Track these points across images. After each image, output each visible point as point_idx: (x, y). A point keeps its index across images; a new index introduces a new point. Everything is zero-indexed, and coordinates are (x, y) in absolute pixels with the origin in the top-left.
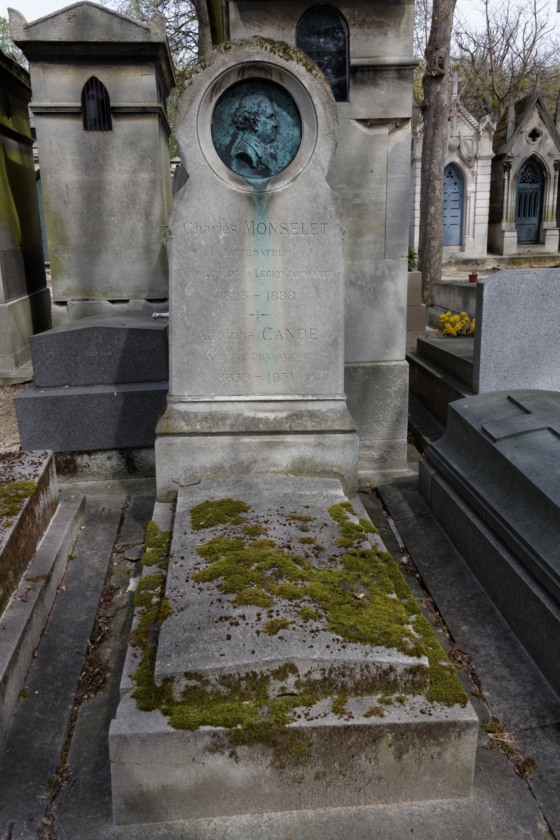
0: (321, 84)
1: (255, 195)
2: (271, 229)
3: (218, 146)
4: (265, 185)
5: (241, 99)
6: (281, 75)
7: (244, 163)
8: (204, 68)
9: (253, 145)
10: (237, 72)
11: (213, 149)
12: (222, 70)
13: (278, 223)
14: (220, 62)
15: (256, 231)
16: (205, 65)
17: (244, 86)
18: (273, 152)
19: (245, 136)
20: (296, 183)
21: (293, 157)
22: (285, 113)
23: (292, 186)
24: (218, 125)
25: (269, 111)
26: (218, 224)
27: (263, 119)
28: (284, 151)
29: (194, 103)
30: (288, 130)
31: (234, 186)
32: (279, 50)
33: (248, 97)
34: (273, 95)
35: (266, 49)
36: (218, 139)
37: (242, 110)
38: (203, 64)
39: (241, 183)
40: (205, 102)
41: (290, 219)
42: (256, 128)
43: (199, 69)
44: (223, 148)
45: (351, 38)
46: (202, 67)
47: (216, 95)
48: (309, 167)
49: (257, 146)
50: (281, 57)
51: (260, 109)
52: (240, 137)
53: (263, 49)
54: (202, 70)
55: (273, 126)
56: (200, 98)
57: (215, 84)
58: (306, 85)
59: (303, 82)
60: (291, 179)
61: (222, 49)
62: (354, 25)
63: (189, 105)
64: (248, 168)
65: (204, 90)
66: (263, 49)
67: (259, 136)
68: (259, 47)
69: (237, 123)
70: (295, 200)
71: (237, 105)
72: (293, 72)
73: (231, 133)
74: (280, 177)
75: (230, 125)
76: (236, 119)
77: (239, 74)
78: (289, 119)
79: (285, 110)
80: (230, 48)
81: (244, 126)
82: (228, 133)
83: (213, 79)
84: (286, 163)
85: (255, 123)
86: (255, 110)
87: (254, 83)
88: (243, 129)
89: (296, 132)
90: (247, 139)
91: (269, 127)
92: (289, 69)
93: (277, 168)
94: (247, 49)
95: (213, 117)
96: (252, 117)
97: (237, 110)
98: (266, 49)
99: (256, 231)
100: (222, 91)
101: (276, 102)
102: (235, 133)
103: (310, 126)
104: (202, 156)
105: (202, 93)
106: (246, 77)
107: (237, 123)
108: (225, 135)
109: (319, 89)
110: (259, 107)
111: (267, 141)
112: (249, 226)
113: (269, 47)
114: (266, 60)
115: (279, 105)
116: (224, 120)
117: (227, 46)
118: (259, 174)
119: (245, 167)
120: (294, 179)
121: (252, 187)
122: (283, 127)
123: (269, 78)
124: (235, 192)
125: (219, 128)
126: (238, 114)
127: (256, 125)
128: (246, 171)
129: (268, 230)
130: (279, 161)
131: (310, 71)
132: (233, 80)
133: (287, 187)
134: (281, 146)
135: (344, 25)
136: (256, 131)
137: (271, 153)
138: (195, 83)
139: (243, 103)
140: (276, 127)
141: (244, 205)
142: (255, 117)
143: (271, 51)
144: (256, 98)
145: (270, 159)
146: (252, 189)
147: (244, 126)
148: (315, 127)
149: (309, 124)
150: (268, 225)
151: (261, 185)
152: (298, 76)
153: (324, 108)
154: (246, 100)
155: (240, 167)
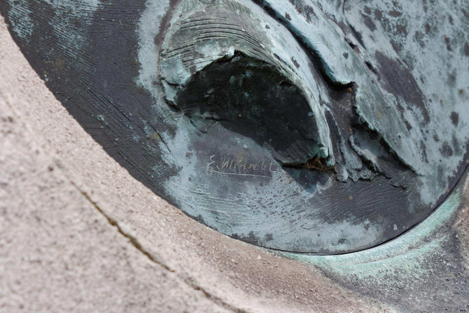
7: (244, 144)
28: (435, 45)
44: (74, 40)
64: (282, 180)
118: (360, 215)
130: (434, 108)
155: (231, 177)
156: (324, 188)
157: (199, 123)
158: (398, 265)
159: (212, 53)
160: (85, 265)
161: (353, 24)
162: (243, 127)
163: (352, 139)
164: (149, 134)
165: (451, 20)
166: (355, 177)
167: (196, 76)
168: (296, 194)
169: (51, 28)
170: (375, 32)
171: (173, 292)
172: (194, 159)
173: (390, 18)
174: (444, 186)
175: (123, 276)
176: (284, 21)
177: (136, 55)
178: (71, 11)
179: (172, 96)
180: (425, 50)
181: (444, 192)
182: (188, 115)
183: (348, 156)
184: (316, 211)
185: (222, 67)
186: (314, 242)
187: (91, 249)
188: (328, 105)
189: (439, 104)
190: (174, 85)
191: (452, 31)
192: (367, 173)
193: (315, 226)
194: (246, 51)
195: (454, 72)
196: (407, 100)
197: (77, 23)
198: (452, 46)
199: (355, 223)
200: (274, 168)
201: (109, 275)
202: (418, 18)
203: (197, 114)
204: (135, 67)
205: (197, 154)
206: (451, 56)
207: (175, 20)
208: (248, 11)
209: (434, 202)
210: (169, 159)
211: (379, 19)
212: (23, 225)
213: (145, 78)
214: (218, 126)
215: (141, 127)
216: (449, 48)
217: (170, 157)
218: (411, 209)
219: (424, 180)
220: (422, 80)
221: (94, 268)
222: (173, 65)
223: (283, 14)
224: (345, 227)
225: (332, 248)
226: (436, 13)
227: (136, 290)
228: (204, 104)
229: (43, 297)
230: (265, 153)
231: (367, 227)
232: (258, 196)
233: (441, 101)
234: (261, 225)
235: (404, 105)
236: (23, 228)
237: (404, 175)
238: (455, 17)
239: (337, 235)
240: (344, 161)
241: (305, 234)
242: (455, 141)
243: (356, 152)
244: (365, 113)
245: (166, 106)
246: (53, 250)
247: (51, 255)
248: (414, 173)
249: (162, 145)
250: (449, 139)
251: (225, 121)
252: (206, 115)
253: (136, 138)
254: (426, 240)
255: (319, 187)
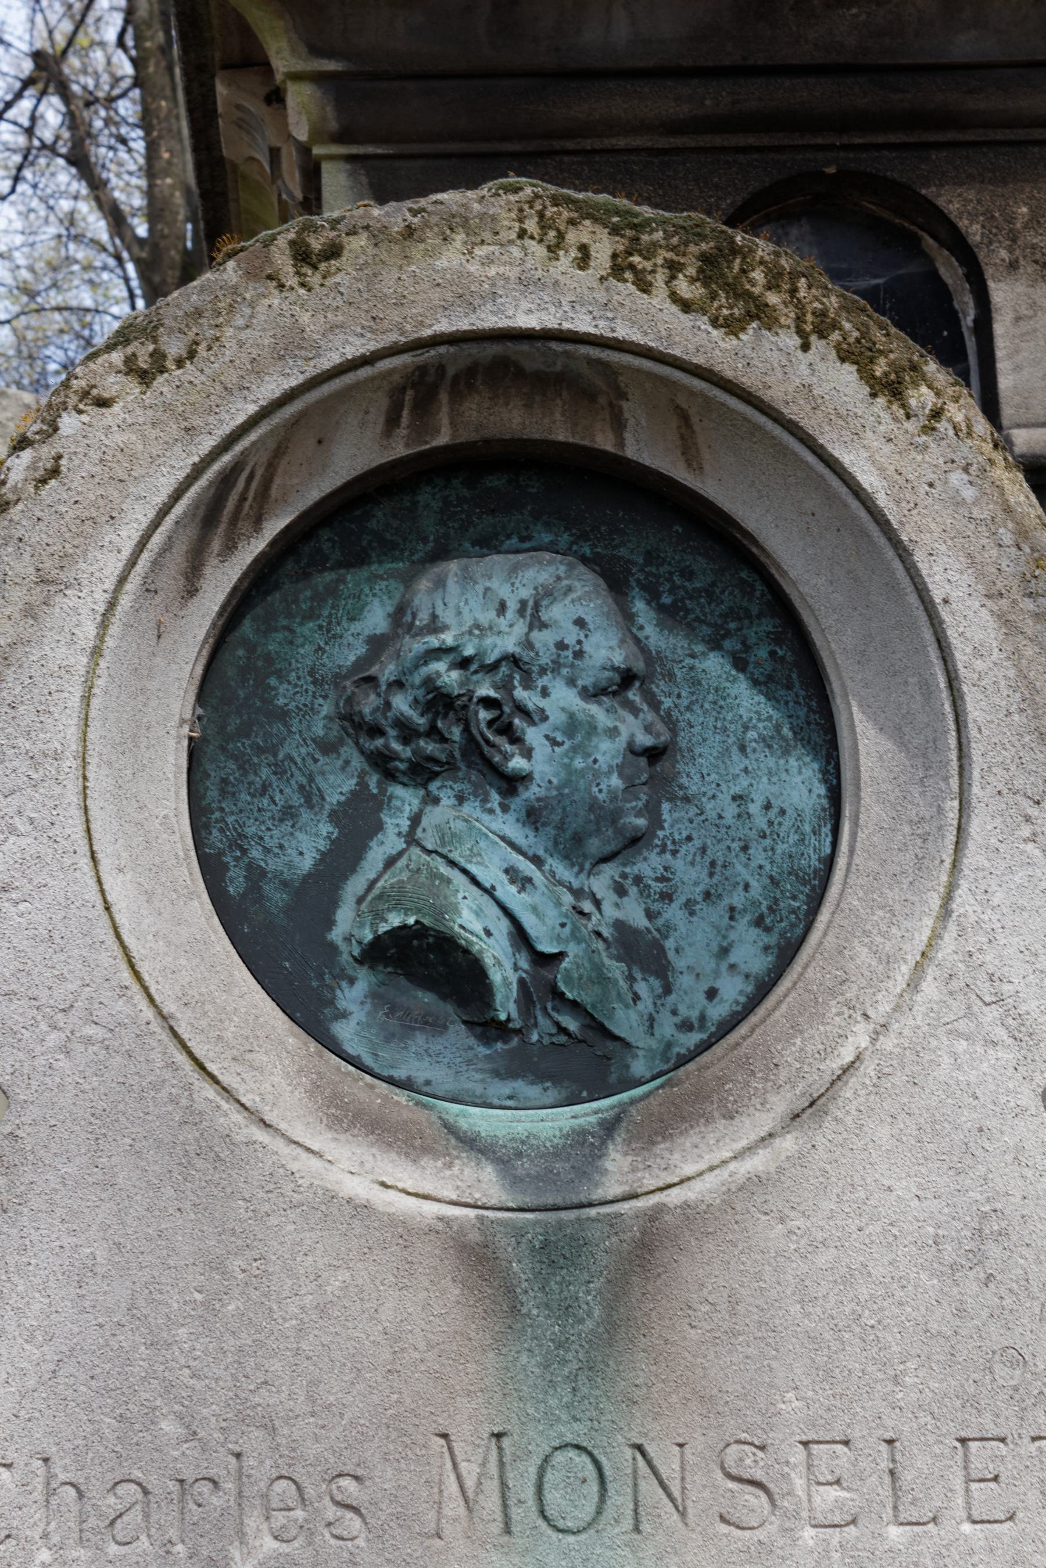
0: (980, 475)
1: (518, 1232)
2: (649, 1486)
3: (236, 883)
4: (586, 1149)
5: (408, 580)
6: (684, 417)
7: (426, 998)
8: (145, 378)
9: (490, 874)
10: (381, 403)
11: (200, 909)
12: (272, 388)
13: (698, 1444)
14: (261, 338)
15: (524, 1514)
16: (158, 356)
17: (428, 498)
18: (638, 919)
19: (433, 817)
20: (825, 1134)
21: (786, 954)
22: (714, 665)
23: (799, 1159)
24: (243, 745)
25: (606, 650)
26: (222, 1466)
27: (561, 699)
28: (716, 913)
29: (71, 599)
30: (743, 766)
31: (356, 1171)
32: (674, 268)
33: (453, 567)
34: (629, 553)
35: (584, 259)
36: (238, 843)
37: (416, 646)
38: (143, 351)
39: (409, 1143)
40: (149, 590)
41: (791, 1405)
42: (518, 763)
43: (112, 384)
44: (277, 897)
45: (1000, 328)
46: (130, 367)
47: (230, 548)
48: (918, 1017)
49: (524, 882)
50: (686, 306)
51: (544, 639)
52: (395, 823)
53: (565, 261)
54: (133, 387)
55: (632, 750)
56: (114, 566)
57: (226, 480)
58: (868, 479)
59: (847, 458)
60: (781, 1104)
61: (282, 259)
62: (1013, 266)
63: (29, 612)
64: (458, 1035)
65: (141, 516)
66: (565, 261)
67: (533, 817)
68: (539, 251)
69: (376, 731)
70: (824, 1259)
71: (376, 618)
72: (775, 394)
73: (334, 798)
74: (700, 1096)
75: (328, 748)
76: (368, 705)
77: (392, 421)
78: (747, 700)
79: (715, 644)
80: (334, 251)
81: (430, 747)
82: (311, 796)
83: (208, 444)
84: (733, 991)
85: (507, 731)
86: (509, 644)
87: (495, 482)
88: (422, 773)
89: (800, 785)
90: (447, 836)
91: (607, 752)
92: (749, 380)
93: (667, 1027)
94: (450, 258)
95: (201, 697)
96: (485, 690)
97: (378, 645)
98: (584, 259)
99: (524, 1514)
100: (275, 526)
101: (653, 596)
102: (360, 795)
103: (902, 744)
104: (109, 957)
105: (129, 535)
106: (443, 439)
107: (376, 731)
108: (288, 813)
109: (959, 503)
110: (537, 623)
111: (594, 846)
112: (470, 1471)
113: (604, 247)
114: (583, 324)
115: (671, 615)
116: (283, 715)
117: (316, 244)
118: (540, 1076)
119: (435, 1026)
120: (811, 1109)
121: (489, 1172)
122: (707, 753)
123: (604, 441)
124: (362, 1209)
125: (245, 766)
126: (388, 672)
127: (516, 739)
128: (443, 1056)
129: (620, 1499)
130: (685, 981)
131: (891, 388)
132: (355, 453)
133: (757, 1163)
134: (690, 876)
135: (950, 271)
136: (511, 784)
137: (619, 925)
138: (79, 470)
139: (423, 599)
140: (654, 754)
141: (430, 1310)
142: (506, 686)
143: (618, 269)
144: (515, 569)
145: (616, 969)
146: (486, 1183)
147: (430, 747)
148: (942, 740)
149: (896, 731)
150: (619, 1459)
151: (557, 1154)
152: (809, 424)
153: (1004, 620)
154: (440, 583)
155: (399, 1024)
156: (506, 1047)
157: (381, 977)
158: (534, 1131)
159: (395, 920)
160: (158, 1091)
161: (595, 889)
162: (428, 983)
163: (549, 1006)
164: (328, 982)
165: (747, 887)
166: (546, 1041)
167: (377, 939)
168: (471, 1048)
169: (261, 887)
170: (625, 899)
171: (222, 1120)
172: (368, 1007)
173: (653, 883)
174: (668, 1062)
175: (184, 1102)
176: (489, 892)
177: (334, 913)
178: (282, 873)
179: (356, 952)
180: (695, 919)
181: (666, 1067)
182: (372, 968)
183: (541, 1019)
184: (488, 1066)
185: (403, 932)
186: (478, 1093)
187: (164, 1081)
188: (525, 971)
189: (693, 977)
190: (360, 943)
191: (743, 899)
192: (563, 1039)
193: (483, 1081)
194: (426, 921)
195: (731, 945)
196: (643, 970)
197: (285, 884)
198: (737, 916)
199: (532, 1084)
200: (452, 1023)
201: (174, 1100)
202: (696, 884)
203: (381, 968)
204: (330, 923)
205: (372, 1003)
206: (732, 927)
207: (379, 884)
208: (449, 881)
209: (648, 1075)
210: (342, 1004)
211: (638, 885)
212: (119, 1059)
213: (336, 935)
214: (403, 981)
215: (321, 976)
216: (732, 918)
217: (344, 1003)
218: (613, 1078)
219: (641, 1053)
220: (677, 951)
221: (163, 1094)
222: (362, 925)
223: (488, 885)
224: (519, 1086)
225: (496, 1102)
226: (727, 879)
227: (192, 1113)
228: (387, 961)
229: (121, 1106)
230: (449, 1009)
231: (545, 1090)
232: (426, 1046)
233: (698, 975)
234: (419, 1070)
235: (638, 976)
236: (118, 1060)
237: (611, 1045)
238: (754, 883)
239: (507, 1091)
240: (536, 1025)
241: (470, 1085)
242: (702, 1018)
243: (550, 1017)
244: (565, 983)
245: (351, 960)
246: (136, 1077)
247: (134, 1080)
248: (627, 1045)
249: (338, 992)
250: (694, 1014)
251: (410, 976)
252: (389, 969)
253: (314, 984)
254: (586, 1115)
255: (499, 1046)
